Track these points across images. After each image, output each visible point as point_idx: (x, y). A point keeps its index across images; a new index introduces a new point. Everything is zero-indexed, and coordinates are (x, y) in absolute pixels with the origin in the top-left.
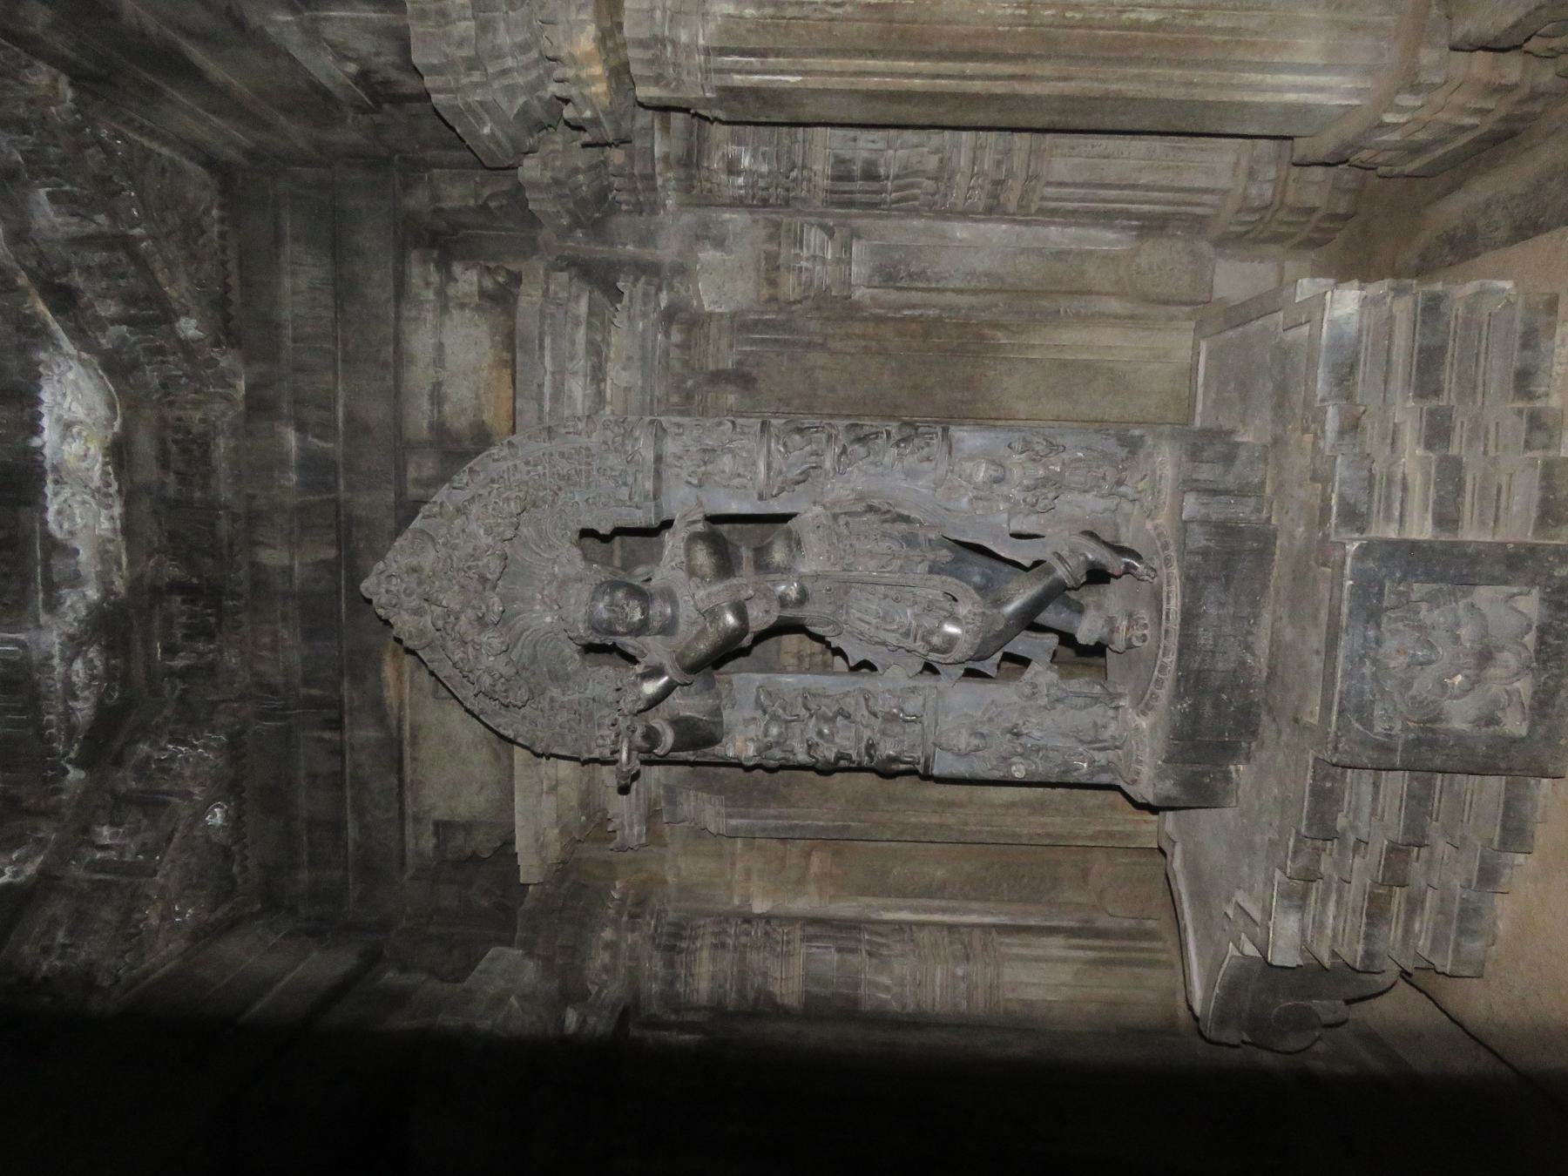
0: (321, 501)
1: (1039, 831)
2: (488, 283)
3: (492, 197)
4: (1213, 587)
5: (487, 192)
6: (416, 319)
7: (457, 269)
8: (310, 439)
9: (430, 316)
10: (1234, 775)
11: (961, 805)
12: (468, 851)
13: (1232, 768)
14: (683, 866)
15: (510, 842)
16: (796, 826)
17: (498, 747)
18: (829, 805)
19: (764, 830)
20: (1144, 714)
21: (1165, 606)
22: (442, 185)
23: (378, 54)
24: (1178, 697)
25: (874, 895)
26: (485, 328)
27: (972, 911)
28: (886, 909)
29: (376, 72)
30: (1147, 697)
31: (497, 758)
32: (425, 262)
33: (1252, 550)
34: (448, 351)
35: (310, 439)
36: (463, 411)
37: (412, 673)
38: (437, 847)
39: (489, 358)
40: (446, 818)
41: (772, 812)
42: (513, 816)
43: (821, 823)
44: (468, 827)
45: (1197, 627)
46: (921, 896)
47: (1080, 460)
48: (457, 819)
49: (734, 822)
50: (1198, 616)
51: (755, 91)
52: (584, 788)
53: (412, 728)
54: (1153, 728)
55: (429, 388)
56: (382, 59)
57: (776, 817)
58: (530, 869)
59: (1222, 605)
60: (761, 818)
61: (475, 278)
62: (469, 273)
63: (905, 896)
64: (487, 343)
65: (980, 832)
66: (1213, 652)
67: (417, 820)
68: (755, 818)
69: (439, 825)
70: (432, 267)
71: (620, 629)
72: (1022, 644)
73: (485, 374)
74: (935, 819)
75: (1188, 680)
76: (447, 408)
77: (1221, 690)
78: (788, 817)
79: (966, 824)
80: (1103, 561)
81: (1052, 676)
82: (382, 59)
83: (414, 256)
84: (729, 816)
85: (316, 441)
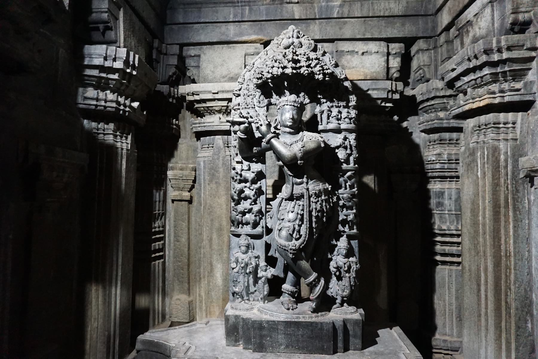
0: (315, 13)
1: (202, 276)
2: (392, 71)
3: (424, 71)
4: (309, 333)
5: (426, 69)
6: (380, 45)
7: (399, 59)
8: (338, 9)
9: (382, 50)
10: (238, 343)
11: (211, 247)
12: (189, 68)
13: (241, 343)
14: (183, 146)
15: (194, 81)
16: (201, 186)
17: (228, 77)
18: (209, 198)
19: (199, 175)
20: (259, 310)
21: (301, 316)
22: (427, 53)
23: (480, 28)
24: (268, 322)
25: (175, 215)
26: (378, 70)
27: (169, 252)
28: (169, 221)
29: (472, 28)
30: (265, 311)
31: (224, 77)
32: (400, 48)
33: (323, 346)
34: (370, 57)
35: (338, 9)
36: (348, 63)
37: (253, 46)
38: (191, 56)
39: (367, 71)
40: (201, 59)
41: (206, 177)
42: (202, 83)
43: (202, 195)
44: (198, 67)
45: (294, 327)
46: (175, 233)
47: (350, 283)
48: (201, 63)
49: (202, 163)
50: (298, 328)
51: (474, 161)
52: (214, 108)
53: (233, 46)
54: (254, 314)
55: (356, 50)
56: (477, 30)
57: (204, 178)
58: (184, 89)
59: (302, 336)
60: (204, 173)
61: (395, 66)
62: (397, 63)
63: (175, 227)
64: (373, 70)
65: (201, 254)
66: (285, 334)
67: (200, 49)
68: (204, 172)
69: (199, 56)
70: (399, 51)
71: (283, 118)
72: (280, 263)
73: (362, 70)
74: (205, 238)
75: (274, 325)
76: (349, 57)
77: (271, 337)
78: (204, 183)
79: (203, 248)
80: (316, 293)
81: (269, 276)
82: (477, 30)
83: (402, 45)
84: (204, 161)
85: (337, 11)
